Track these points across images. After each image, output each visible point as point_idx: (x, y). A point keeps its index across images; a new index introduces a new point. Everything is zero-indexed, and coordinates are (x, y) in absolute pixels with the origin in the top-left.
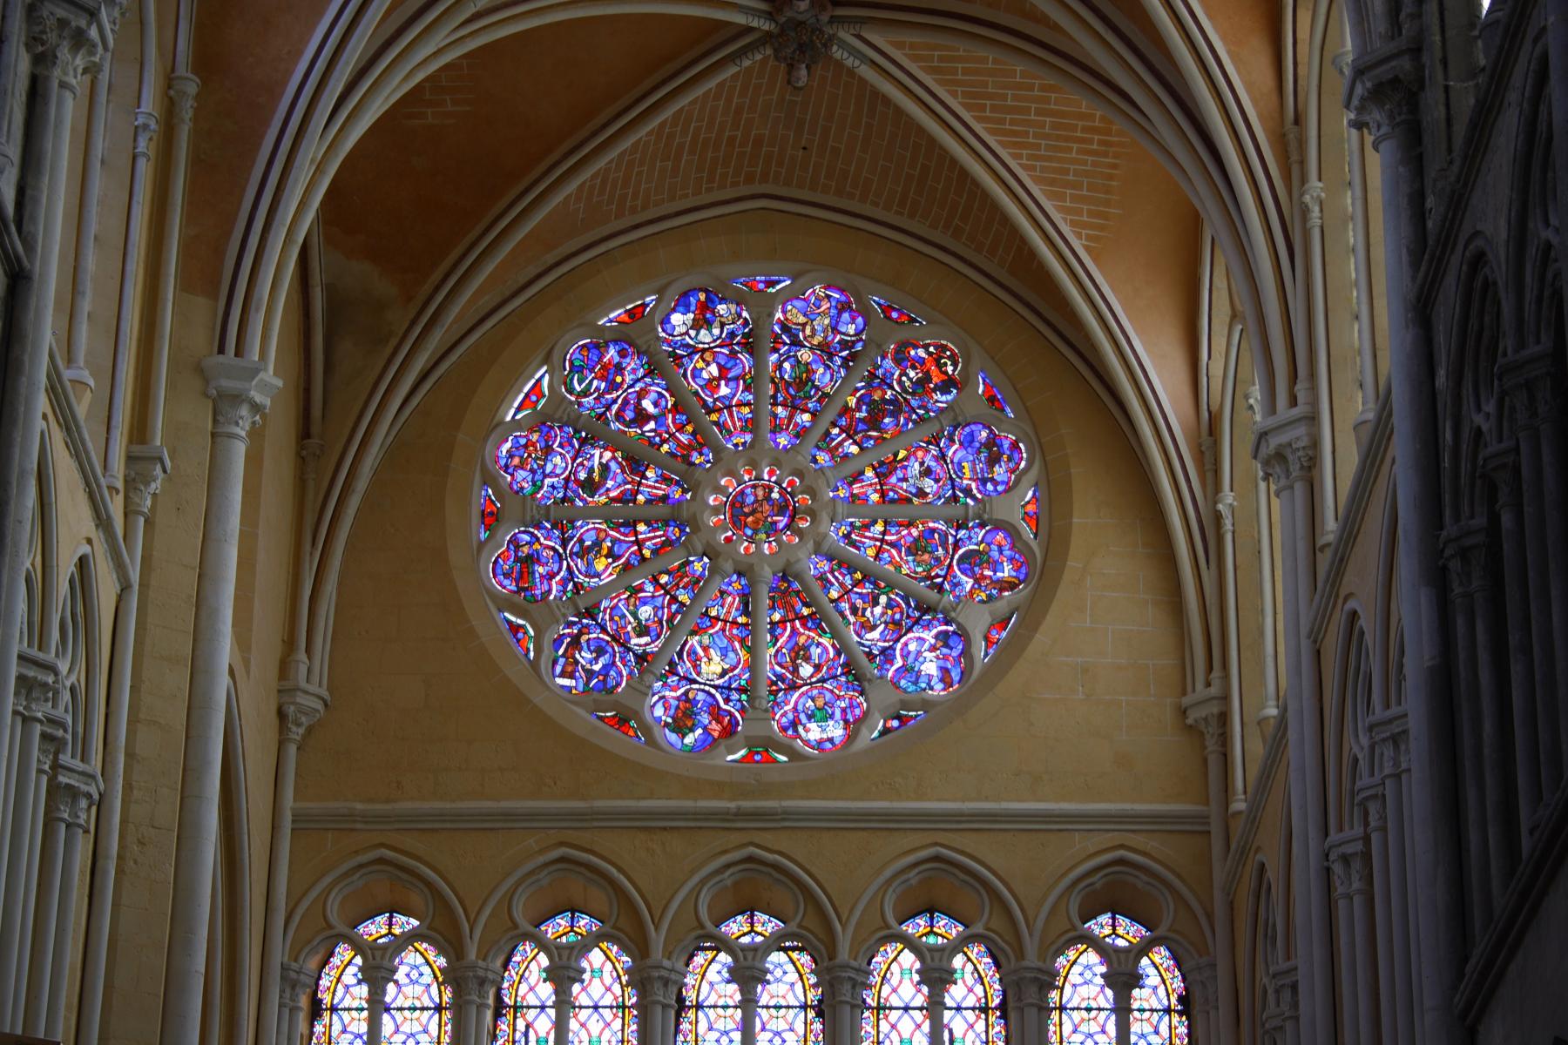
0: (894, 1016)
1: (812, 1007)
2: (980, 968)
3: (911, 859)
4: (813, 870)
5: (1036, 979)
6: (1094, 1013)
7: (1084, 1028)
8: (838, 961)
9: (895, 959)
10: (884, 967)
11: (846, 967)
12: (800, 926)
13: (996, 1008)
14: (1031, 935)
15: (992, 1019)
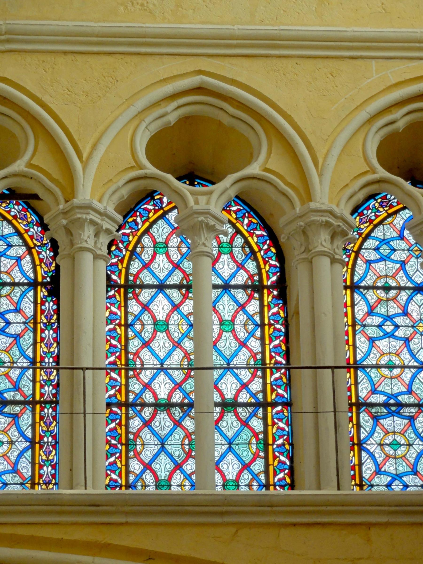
0: (145, 295)
1: (43, 284)
2: (253, 241)
3: (169, 88)
4: (46, 99)
5: (327, 224)
6: (392, 293)
7: (381, 309)
8: (79, 200)
9: (147, 231)
10: (133, 240)
11: (89, 207)
12: (30, 165)
13: (273, 286)
14: (320, 175)
15: (267, 299)
